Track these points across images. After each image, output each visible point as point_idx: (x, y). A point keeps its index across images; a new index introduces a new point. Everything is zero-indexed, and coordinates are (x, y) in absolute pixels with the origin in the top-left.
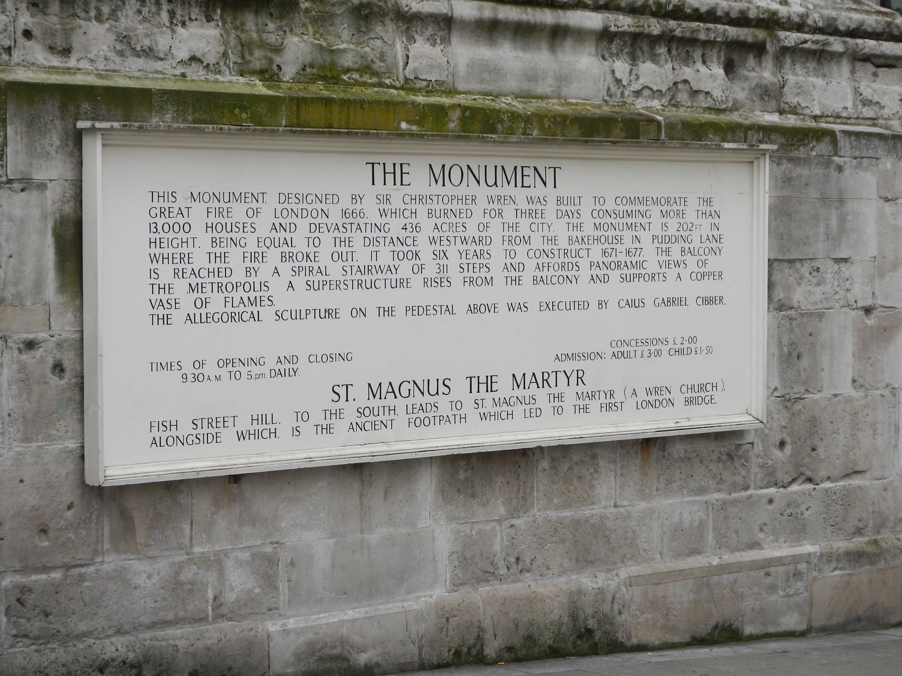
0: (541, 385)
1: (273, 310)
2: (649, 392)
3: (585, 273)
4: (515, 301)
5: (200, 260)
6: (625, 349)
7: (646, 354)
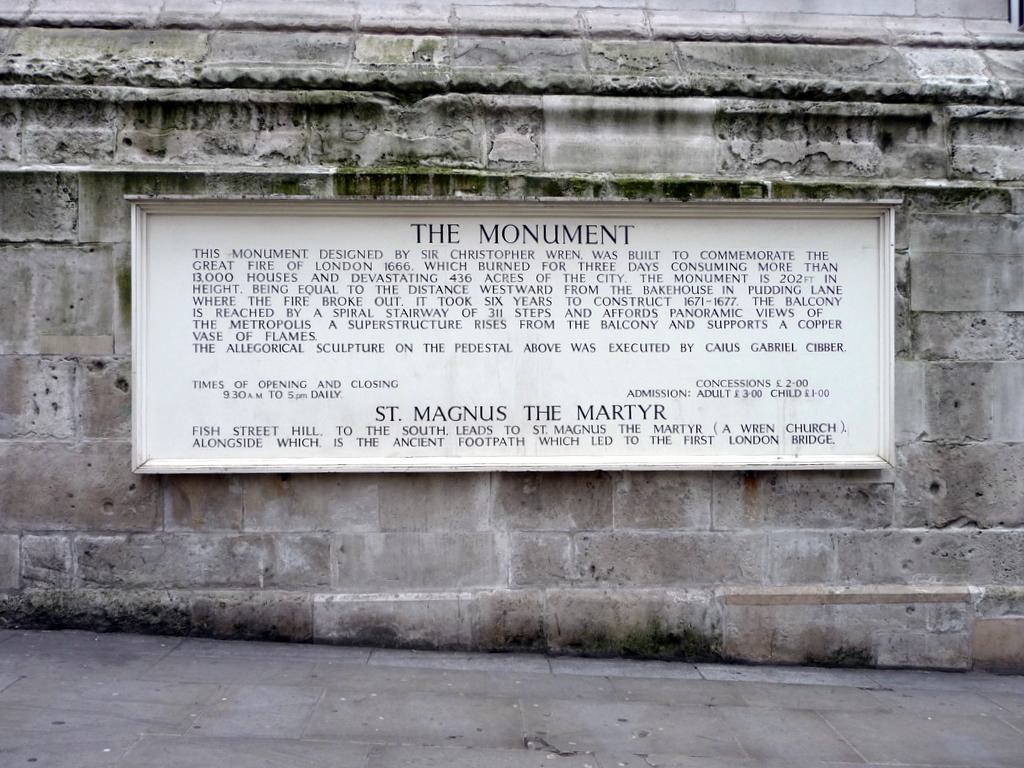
0: (611, 416)
1: (315, 343)
2: (745, 428)
3: (664, 317)
4: (580, 342)
5: (242, 302)
6: (715, 388)
7: (741, 393)
